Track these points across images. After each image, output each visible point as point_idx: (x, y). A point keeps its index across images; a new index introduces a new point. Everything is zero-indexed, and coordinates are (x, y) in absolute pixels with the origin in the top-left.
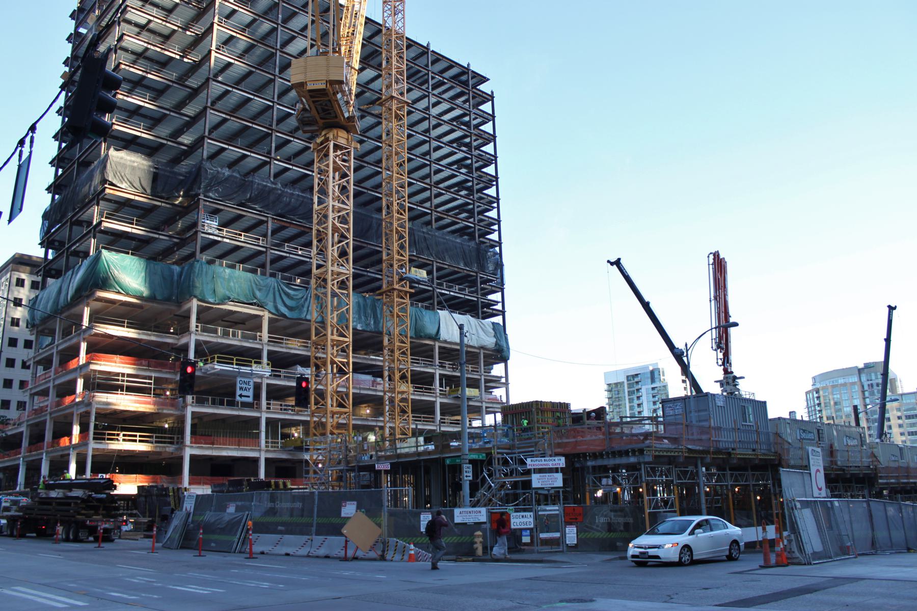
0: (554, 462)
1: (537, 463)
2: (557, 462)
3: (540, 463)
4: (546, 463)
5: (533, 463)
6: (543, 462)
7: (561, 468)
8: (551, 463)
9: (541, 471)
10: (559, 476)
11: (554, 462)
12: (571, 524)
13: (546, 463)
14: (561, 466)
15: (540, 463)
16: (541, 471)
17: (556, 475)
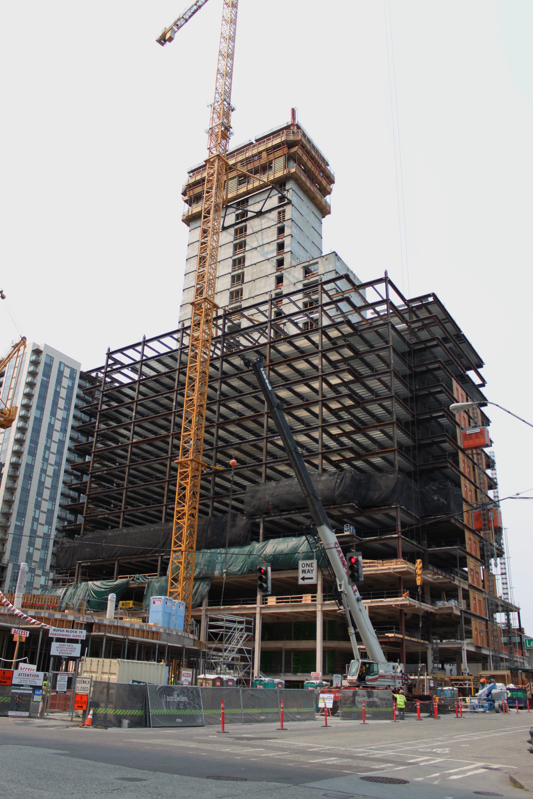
0: (75, 634)
1: (59, 633)
2: (78, 634)
3: (62, 633)
4: (68, 633)
5: (55, 632)
6: (65, 633)
7: (82, 640)
8: (72, 634)
9: (59, 640)
10: (78, 647)
11: (75, 634)
12: (82, 696)
13: (68, 633)
14: (82, 638)
15: (62, 633)
16: (59, 640)
17: (75, 645)
